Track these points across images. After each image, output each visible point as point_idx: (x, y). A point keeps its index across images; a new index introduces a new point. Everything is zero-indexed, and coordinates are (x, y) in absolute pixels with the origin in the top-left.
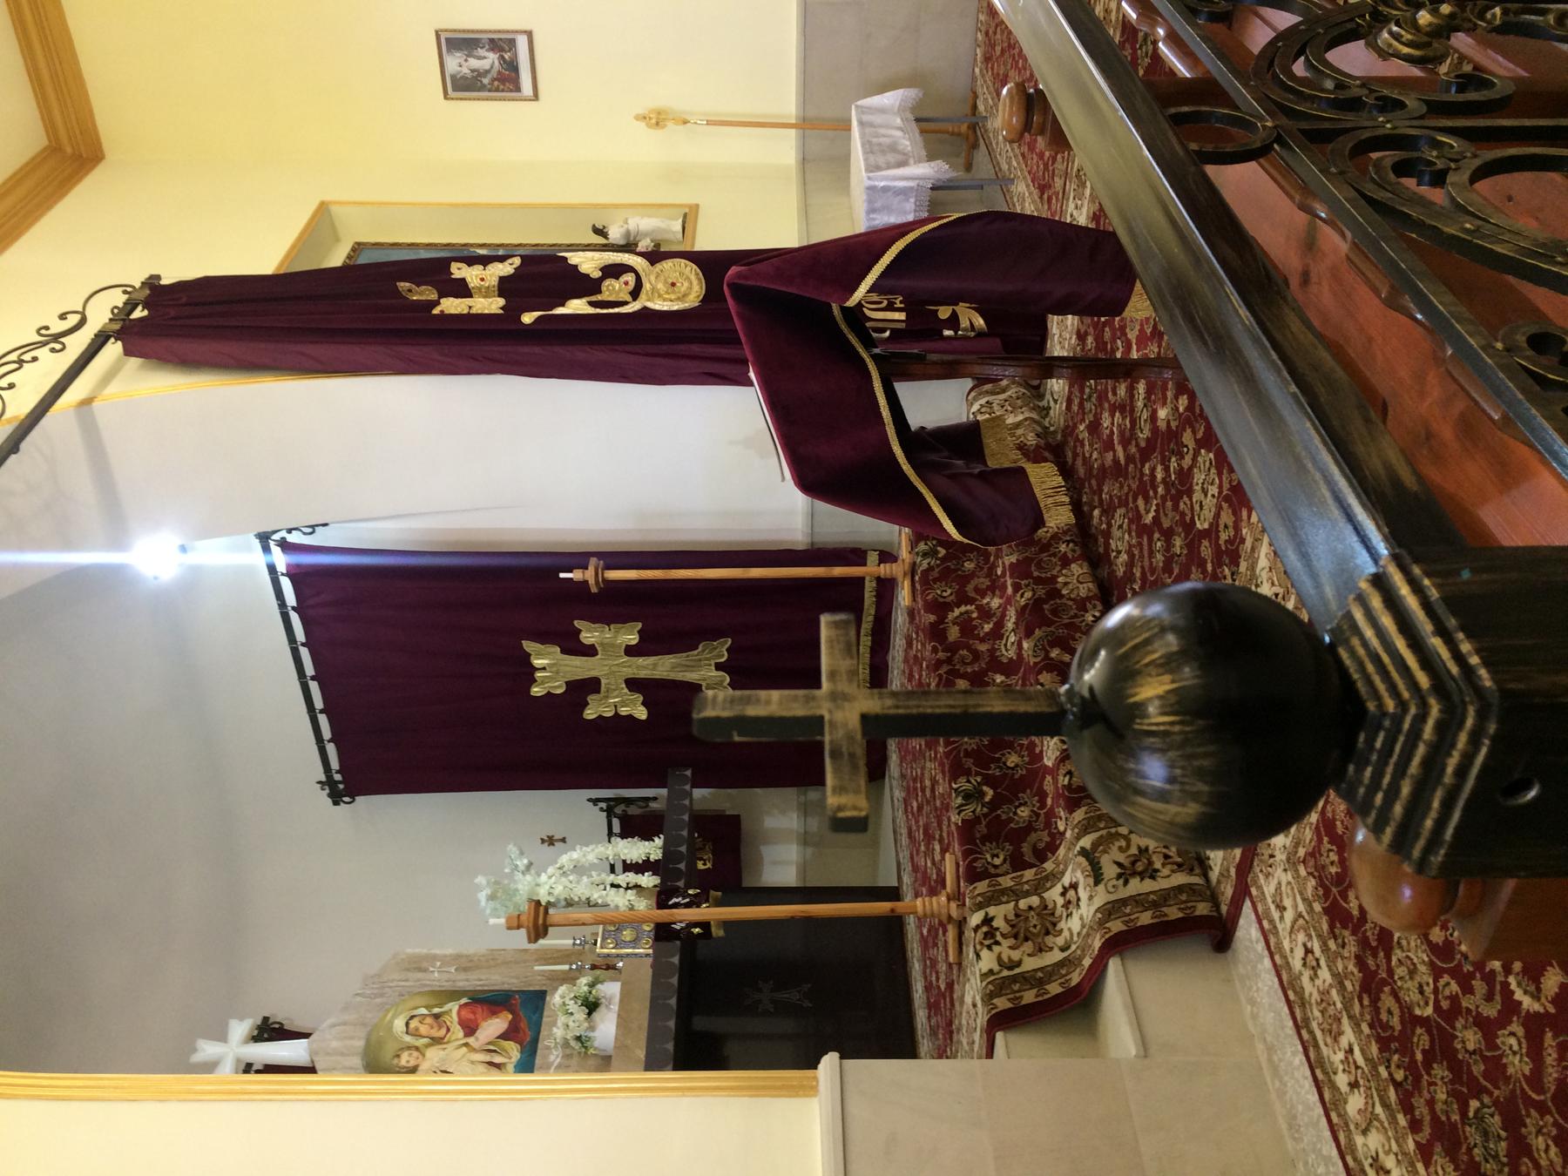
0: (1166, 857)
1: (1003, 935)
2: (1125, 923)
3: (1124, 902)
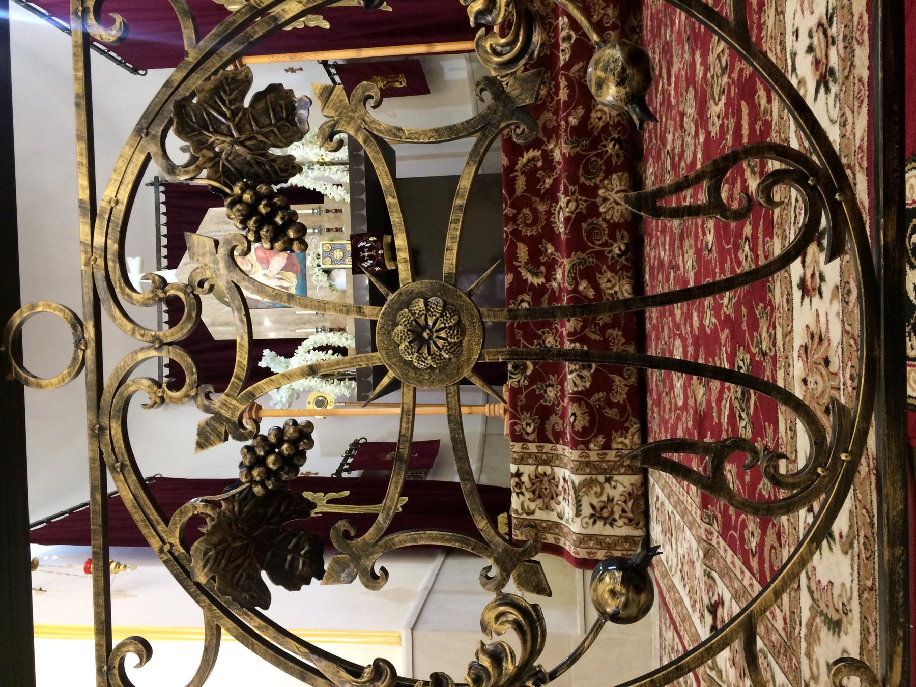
0: (624, 511)
1: (527, 489)
2: (588, 553)
3: (590, 537)
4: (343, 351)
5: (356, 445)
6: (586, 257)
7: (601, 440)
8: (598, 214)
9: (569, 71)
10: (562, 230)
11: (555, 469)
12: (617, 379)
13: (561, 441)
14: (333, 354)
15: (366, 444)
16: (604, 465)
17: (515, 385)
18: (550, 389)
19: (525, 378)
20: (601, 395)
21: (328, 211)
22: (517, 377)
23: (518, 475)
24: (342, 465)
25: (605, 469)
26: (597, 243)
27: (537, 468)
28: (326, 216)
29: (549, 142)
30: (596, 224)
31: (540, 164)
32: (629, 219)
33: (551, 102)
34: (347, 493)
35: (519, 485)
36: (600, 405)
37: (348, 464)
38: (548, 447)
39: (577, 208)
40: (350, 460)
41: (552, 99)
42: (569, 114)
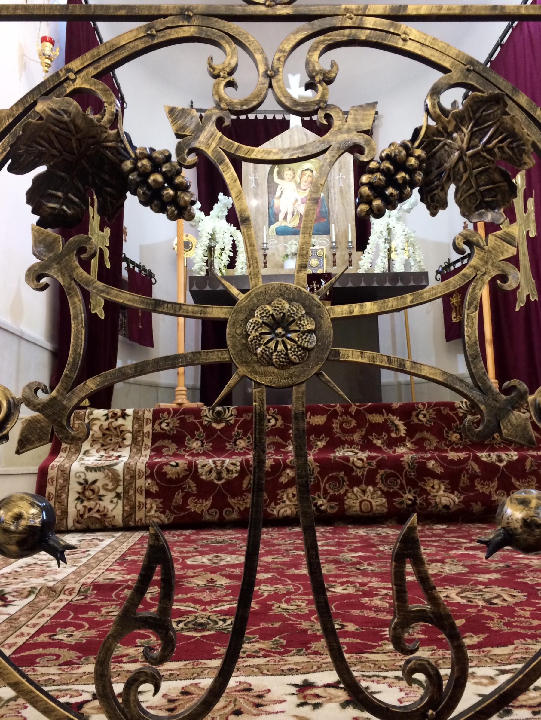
0: (90, 510)
1: (111, 423)
2: (52, 478)
3: (67, 480)
4: (232, 264)
5: (150, 275)
6: (314, 476)
7: (155, 489)
8: (351, 486)
9: (473, 460)
10: (337, 454)
11: (128, 449)
12: (208, 503)
13: (153, 453)
14: (229, 256)
15: (151, 284)
16: (132, 492)
17: (203, 413)
18: (200, 443)
19: (209, 422)
20: (195, 489)
21: (350, 254)
22: (210, 415)
23: (124, 416)
24: (133, 263)
25: (128, 492)
26: (327, 485)
27: (129, 432)
28: (346, 253)
29: (412, 443)
30: (343, 484)
31: (393, 435)
32: (347, 513)
33: (445, 444)
34: (108, 266)
35: (115, 416)
36: (185, 488)
37: (134, 267)
38: (148, 441)
39: (357, 467)
40: (137, 270)
41: (448, 446)
42: (436, 460)
